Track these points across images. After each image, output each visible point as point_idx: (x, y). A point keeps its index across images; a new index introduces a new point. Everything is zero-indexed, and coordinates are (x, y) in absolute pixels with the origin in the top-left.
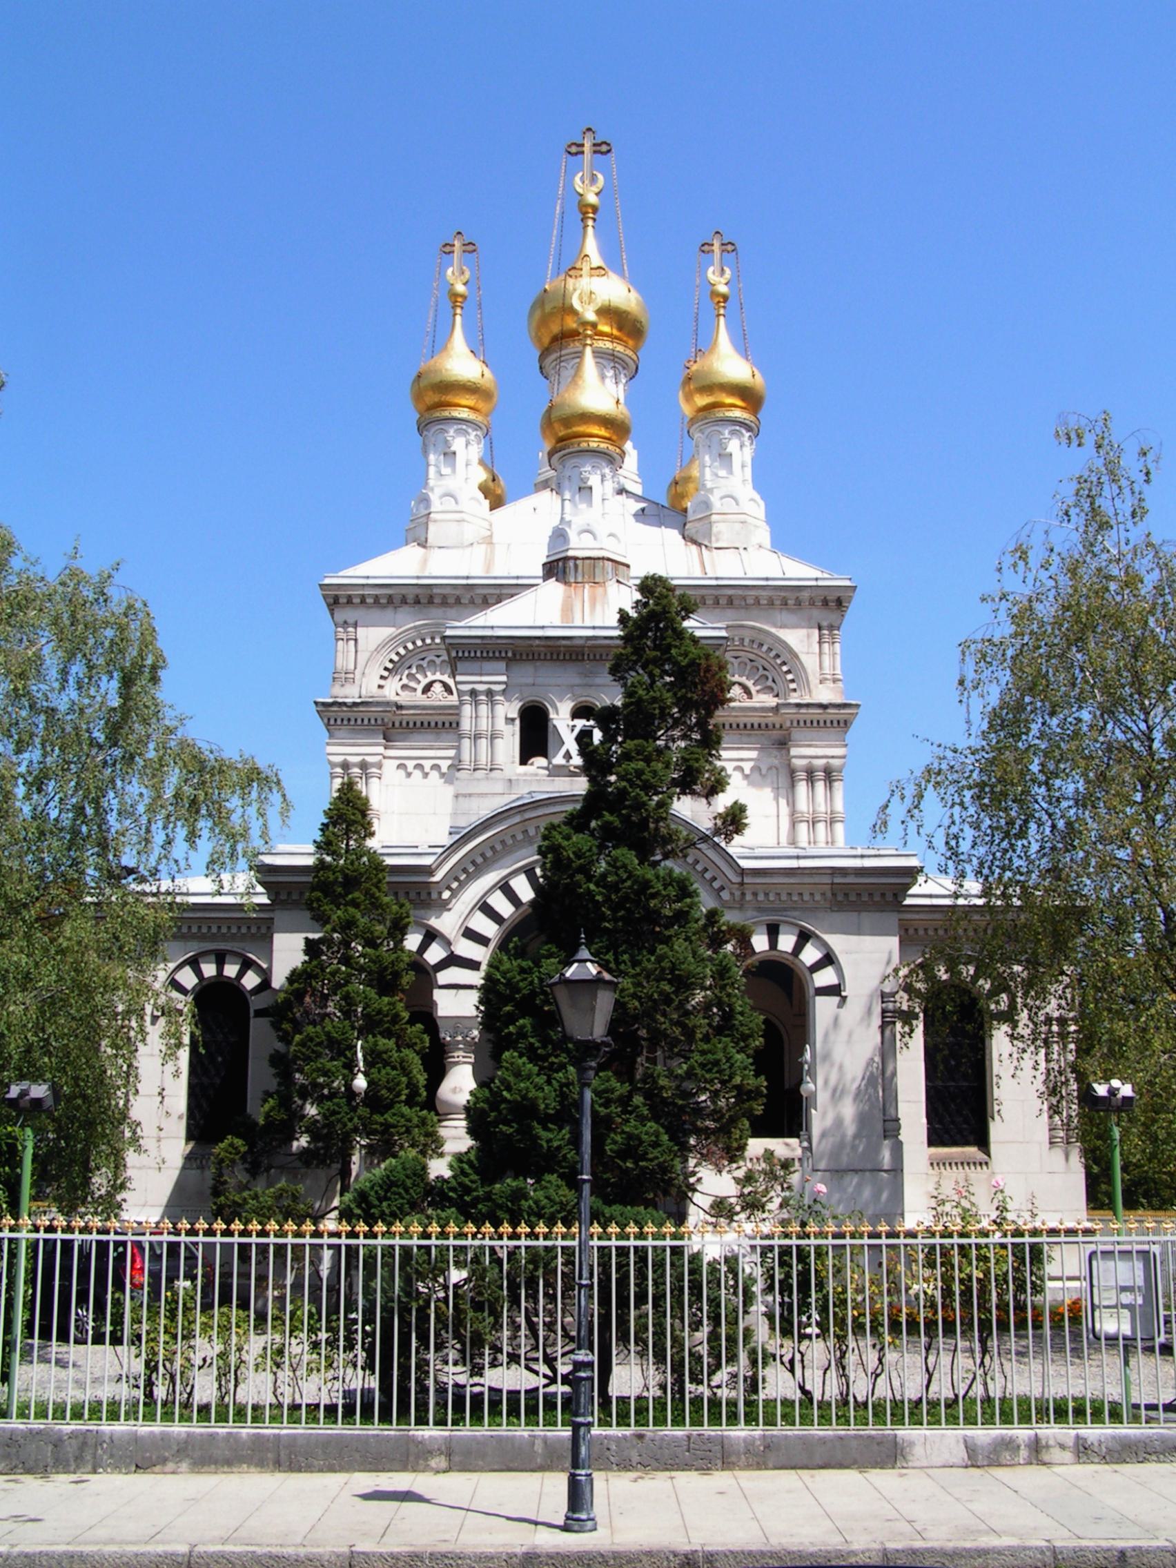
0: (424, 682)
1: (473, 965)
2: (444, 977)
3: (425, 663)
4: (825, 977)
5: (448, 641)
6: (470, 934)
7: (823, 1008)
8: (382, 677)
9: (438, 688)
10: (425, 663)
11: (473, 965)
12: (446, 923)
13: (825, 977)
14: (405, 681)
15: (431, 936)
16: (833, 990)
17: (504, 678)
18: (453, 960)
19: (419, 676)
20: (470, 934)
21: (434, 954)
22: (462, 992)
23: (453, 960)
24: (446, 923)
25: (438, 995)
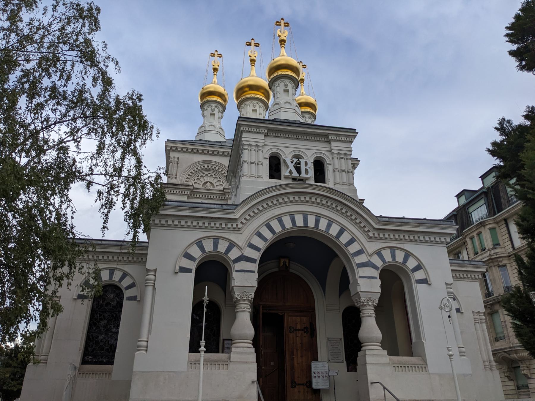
0: (204, 182)
1: (251, 260)
2: (238, 266)
3: (204, 175)
4: (419, 275)
5: (239, 122)
6: (251, 246)
7: (420, 290)
8: (187, 178)
9: (208, 184)
10: (204, 175)
11: (251, 260)
12: (240, 239)
13: (419, 275)
14: (196, 181)
15: (232, 245)
16: (424, 281)
17: (263, 141)
18: (242, 258)
19: (202, 179)
20: (251, 246)
21: (234, 254)
22: (246, 273)
23: (242, 258)
24: (240, 239)
25: (234, 275)
